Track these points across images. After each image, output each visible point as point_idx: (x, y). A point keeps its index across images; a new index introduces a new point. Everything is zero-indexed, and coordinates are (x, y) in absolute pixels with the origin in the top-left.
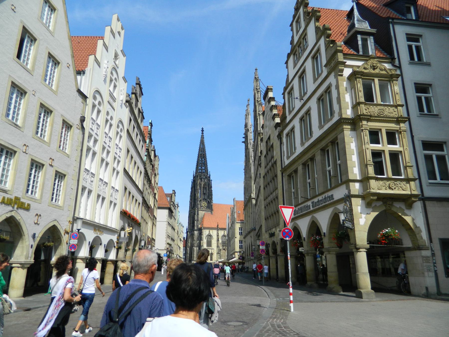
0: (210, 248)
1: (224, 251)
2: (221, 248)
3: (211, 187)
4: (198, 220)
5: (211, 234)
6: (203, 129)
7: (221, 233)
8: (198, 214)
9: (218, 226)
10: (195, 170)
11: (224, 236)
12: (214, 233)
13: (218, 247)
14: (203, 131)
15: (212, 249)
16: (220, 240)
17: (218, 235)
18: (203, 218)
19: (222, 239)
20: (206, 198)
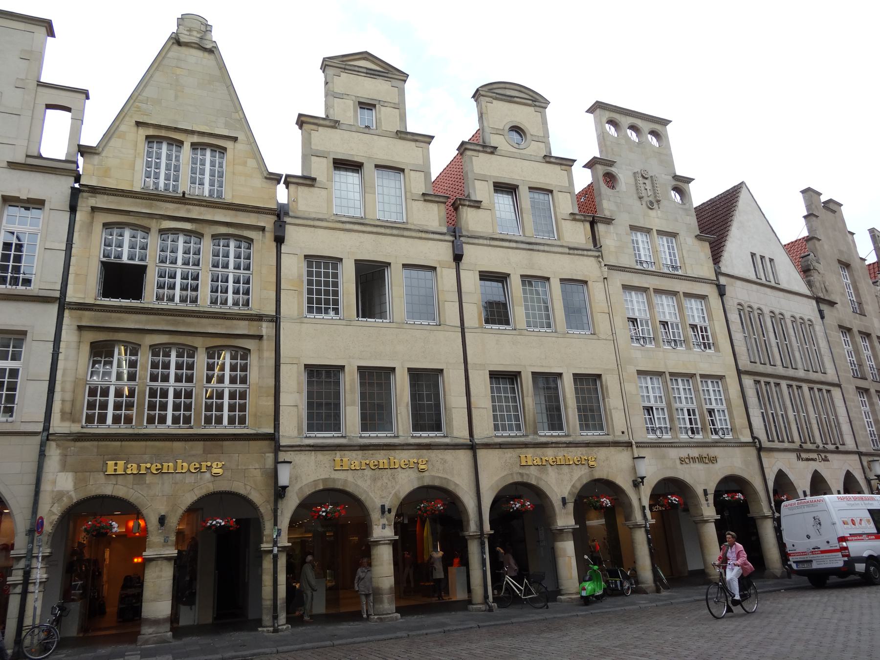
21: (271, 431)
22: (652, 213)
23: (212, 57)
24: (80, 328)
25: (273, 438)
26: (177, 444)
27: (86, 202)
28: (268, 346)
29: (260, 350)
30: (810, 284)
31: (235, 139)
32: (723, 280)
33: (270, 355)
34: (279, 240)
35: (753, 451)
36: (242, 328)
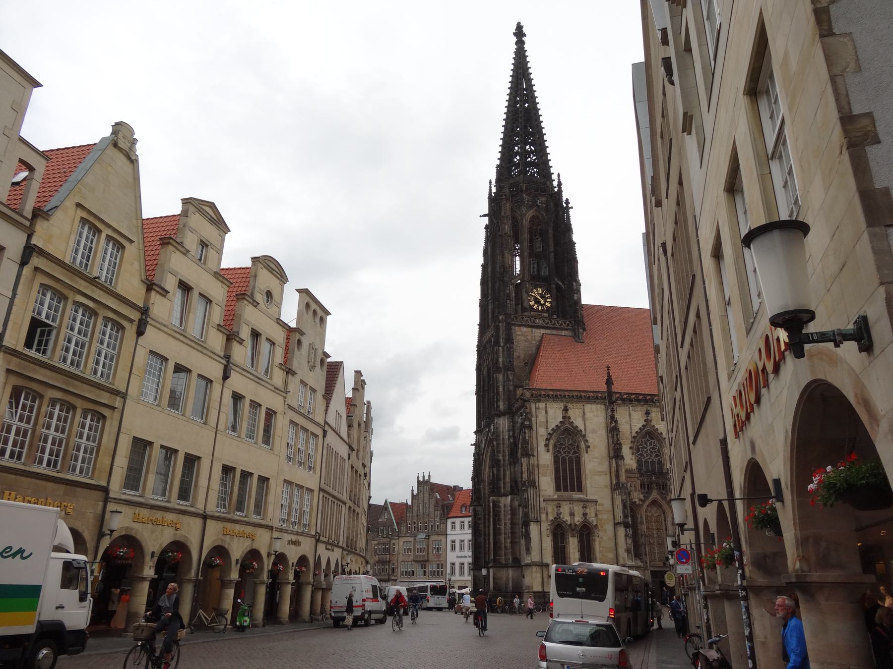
0: (577, 495)
1: (655, 511)
2: (637, 496)
3: (568, 229)
4: (509, 367)
5: (579, 423)
6: (519, 28)
7: (631, 420)
8: (509, 340)
9: (609, 382)
10: (493, 177)
11: (648, 434)
12: (591, 420)
13: (617, 487)
14: (519, 33)
15: (585, 502)
16: (626, 451)
17: (613, 430)
18: (532, 362)
19: (636, 449)
20: (545, 271)
21: (105, 484)
22: (311, 374)
23: (131, 166)
24: (9, 371)
25: (105, 490)
26: (50, 485)
27: (36, 261)
28: (117, 415)
29: (112, 418)
30: (349, 435)
31: (131, 241)
32: (327, 428)
33: (116, 423)
34: (140, 333)
35: (314, 540)
36: (105, 398)
